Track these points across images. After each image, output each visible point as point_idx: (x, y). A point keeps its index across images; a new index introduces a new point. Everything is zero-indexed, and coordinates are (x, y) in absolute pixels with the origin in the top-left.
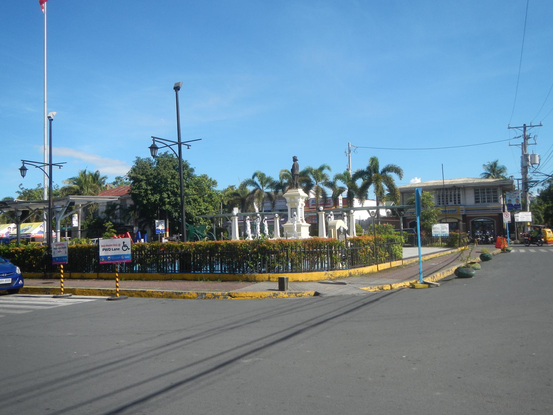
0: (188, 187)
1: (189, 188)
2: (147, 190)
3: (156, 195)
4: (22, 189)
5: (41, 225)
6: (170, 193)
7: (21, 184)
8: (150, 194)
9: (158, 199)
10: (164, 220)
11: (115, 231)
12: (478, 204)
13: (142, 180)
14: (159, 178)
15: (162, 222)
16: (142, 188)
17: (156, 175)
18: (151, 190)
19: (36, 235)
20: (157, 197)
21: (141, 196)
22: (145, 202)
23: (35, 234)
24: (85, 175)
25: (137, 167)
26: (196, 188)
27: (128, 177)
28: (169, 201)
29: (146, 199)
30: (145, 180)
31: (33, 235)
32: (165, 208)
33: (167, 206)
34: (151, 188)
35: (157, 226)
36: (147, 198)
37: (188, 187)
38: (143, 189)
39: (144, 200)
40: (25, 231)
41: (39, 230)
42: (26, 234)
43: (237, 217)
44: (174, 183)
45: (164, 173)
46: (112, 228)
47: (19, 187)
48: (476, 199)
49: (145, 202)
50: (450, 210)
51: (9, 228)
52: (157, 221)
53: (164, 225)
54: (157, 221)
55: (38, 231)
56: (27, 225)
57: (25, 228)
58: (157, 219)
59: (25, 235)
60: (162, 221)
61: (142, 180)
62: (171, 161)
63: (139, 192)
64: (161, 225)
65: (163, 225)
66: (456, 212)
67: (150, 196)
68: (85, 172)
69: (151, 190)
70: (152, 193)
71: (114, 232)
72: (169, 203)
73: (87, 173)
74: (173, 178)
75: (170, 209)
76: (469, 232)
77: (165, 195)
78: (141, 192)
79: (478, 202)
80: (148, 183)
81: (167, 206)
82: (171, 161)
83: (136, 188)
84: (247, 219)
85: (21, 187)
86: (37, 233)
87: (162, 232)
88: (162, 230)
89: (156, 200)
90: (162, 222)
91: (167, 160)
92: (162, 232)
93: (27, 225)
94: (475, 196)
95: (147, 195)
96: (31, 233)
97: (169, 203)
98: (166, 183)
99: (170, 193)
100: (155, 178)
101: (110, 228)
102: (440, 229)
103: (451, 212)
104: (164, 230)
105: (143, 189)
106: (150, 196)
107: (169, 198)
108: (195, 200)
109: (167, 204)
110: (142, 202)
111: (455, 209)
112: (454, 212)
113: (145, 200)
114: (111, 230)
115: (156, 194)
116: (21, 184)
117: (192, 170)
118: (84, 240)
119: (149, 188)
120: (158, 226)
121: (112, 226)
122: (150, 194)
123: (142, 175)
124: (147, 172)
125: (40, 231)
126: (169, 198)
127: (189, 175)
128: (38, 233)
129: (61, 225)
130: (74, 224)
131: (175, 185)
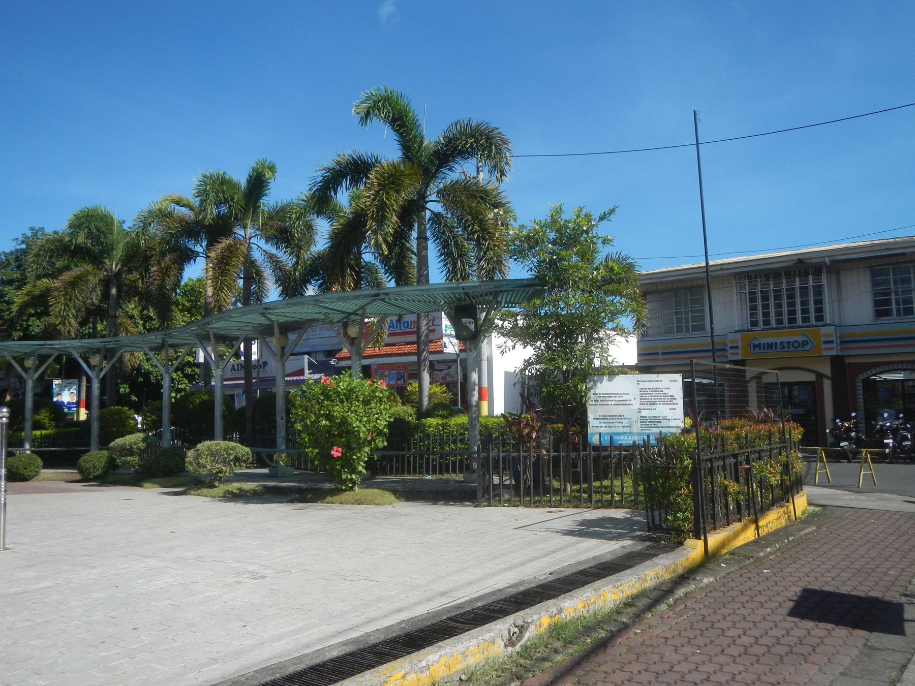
10: (76, 381)
12: (884, 320)
15: (70, 383)
35: (58, 394)
48: (877, 303)
50: (788, 343)
52: (56, 382)
53: (75, 392)
54: (56, 382)
58: (57, 377)
60: (70, 381)
64: (69, 390)
65: (74, 389)
66: (807, 348)
76: (853, 414)
79: (888, 313)
87: (69, 408)
88: (69, 403)
90: (70, 383)
92: (69, 408)
94: (875, 295)
102: (636, 405)
103: (792, 349)
104: (73, 403)
111: (805, 338)
112: (801, 349)
120: (61, 394)
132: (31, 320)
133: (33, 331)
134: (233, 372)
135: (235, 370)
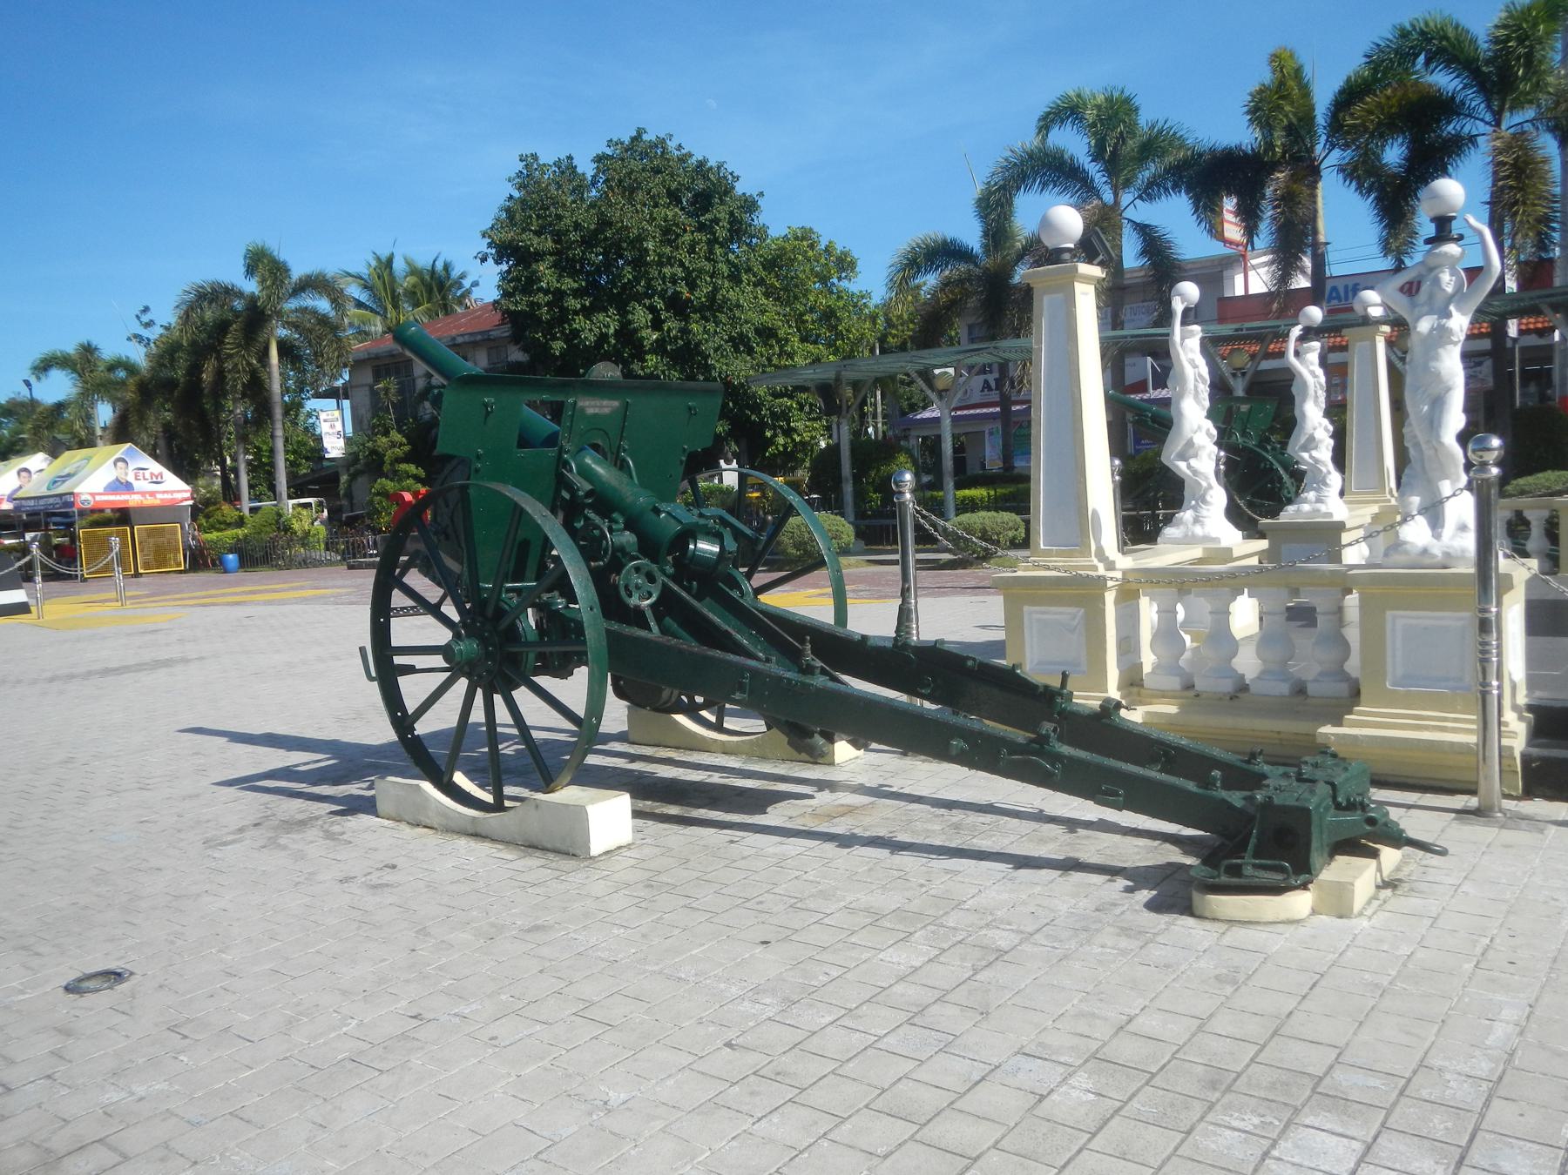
0: (735, 278)
1: (741, 282)
2: (559, 295)
3: (601, 316)
4: (148, 325)
5: (118, 455)
6: (660, 305)
7: (146, 310)
8: (576, 313)
9: (612, 331)
11: (421, 472)
13: (539, 256)
14: (606, 239)
16: (540, 289)
17: (593, 227)
18: (577, 293)
19: (98, 498)
20: (609, 322)
21: (539, 320)
22: (558, 346)
23: (93, 495)
24: (391, 274)
25: (523, 201)
26: (772, 286)
27: (489, 250)
28: (657, 340)
29: (563, 333)
30: (551, 254)
31: (83, 498)
32: (643, 369)
33: (652, 360)
34: (576, 285)
36: (565, 328)
37: (735, 278)
38: (546, 292)
39: (554, 338)
40: (64, 481)
41: (114, 478)
42: (60, 496)
43: (1096, 271)
44: (670, 261)
45: (631, 218)
46: (407, 459)
47: (138, 317)
49: (558, 346)
51: (23, 474)
55: (105, 485)
56: (76, 460)
57: (66, 471)
59: (58, 500)
61: (539, 256)
62: (657, 171)
63: (532, 304)
67: (579, 322)
68: (390, 261)
69: (577, 293)
70: (583, 306)
71: (417, 478)
72: (659, 348)
73: (399, 266)
74: (669, 234)
75: (663, 372)
77: (640, 316)
78: (539, 306)
80: (565, 265)
81: (652, 360)
82: (657, 171)
83: (515, 289)
84: (1178, 306)
85: (145, 319)
89: (603, 338)
91: (643, 170)
93: (76, 460)
95: (563, 316)
96: (76, 491)
97: (659, 348)
98: (639, 263)
99: (660, 305)
100: (589, 241)
101: (398, 460)
105: (546, 292)
106: (579, 322)
107: (657, 324)
108: (766, 333)
109: (649, 352)
110: (546, 348)
113: (558, 339)
114: (403, 466)
115: (606, 310)
116: (146, 310)
117: (750, 205)
118: (299, 513)
119: (569, 284)
121: (407, 448)
122: (576, 313)
123: (538, 233)
124: (559, 218)
125: (117, 479)
126: (657, 324)
127: (738, 229)
129: (287, 452)
130: (329, 450)
131: (679, 272)
132: (577, 321)
133: (586, 338)
134: (986, 391)
135: (990, 389)
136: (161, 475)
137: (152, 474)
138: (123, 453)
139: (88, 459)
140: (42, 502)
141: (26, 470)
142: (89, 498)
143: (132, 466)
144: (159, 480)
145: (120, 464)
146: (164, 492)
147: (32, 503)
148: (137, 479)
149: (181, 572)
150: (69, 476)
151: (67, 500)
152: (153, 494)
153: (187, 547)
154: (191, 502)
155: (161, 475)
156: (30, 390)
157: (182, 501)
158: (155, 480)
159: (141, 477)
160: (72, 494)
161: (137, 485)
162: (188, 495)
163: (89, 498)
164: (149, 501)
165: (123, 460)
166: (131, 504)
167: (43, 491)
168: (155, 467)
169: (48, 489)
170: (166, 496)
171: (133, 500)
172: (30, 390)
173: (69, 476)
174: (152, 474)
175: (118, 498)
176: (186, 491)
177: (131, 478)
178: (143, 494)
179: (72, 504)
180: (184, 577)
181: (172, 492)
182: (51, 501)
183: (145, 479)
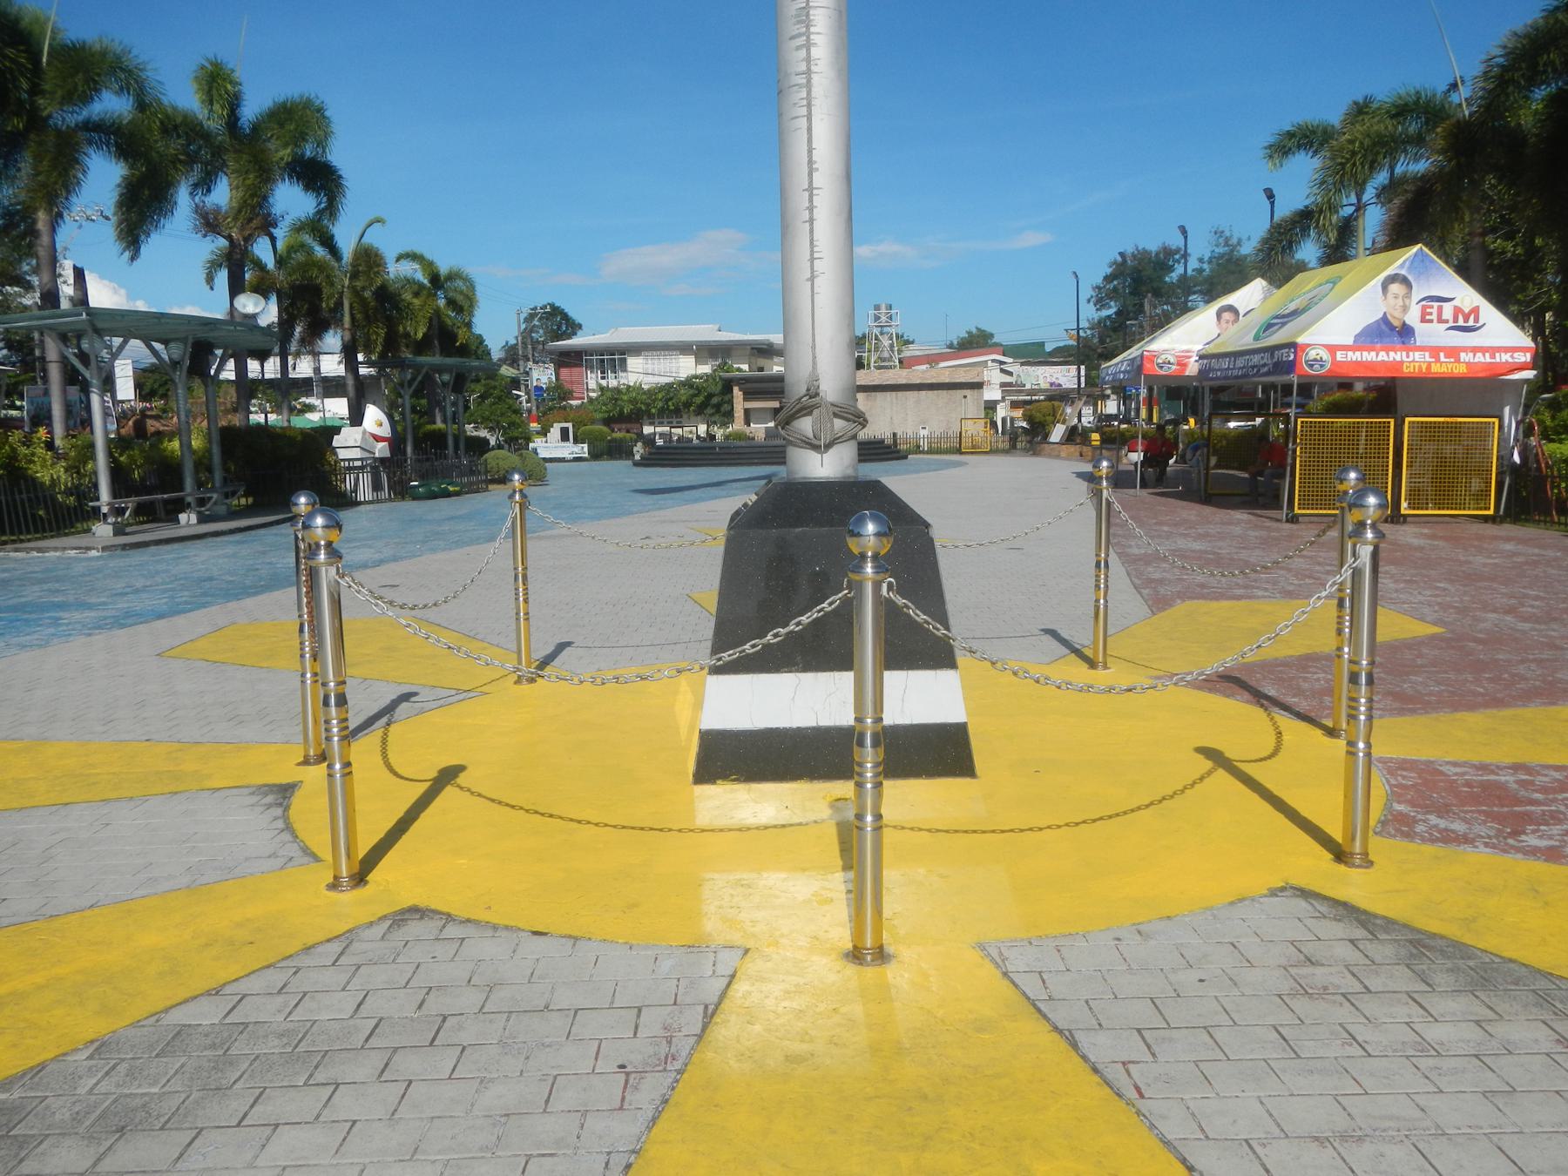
23: (1332, 349)
31: (1312, 354)
40: (1284, 324)
41: (1380, 315)
51: (1227, 316)
57: (1292, 307)
59: (1267, 359)
86: (1350, 341)
96: (1300, 340)
125: (1385, 319)
128: (1357, 337)
136: (1476, 311)
137: (1457, 311)
138: (1402, 266)
139: (1334, 282)
140: (1240, 362)
141: (1231, 309)
142: (1325, 355)
143: (1418, 294)
144: (1471, 323)
145: (1395, 288)
146: (1475, 350)
147: (1225, 364)
148: (1423, 320)
149: (1486, 519)
150: (1295, 313)
151: (1282, 358)
152: (1453, 352)
153: (1506, 467)
154: (1530, 374)
155: (1476, 311)
156: (1272, 204)
157: (1512, 371)
158: (1461, 323)
159: (1434, 317)
160: (1293, 345)
161: (1432, 334)
162: (1526, 358)
163: (1325, 355)
164: (1444, 367)
165: (1405, 281)
166: (1407, 370)
167: (1247, 342)
168: (1466, 296)
169: (1256, 338)
170: (1479, 358)
171: (1412, 362)
172: (1272, 204)
173: (1295, 313)
174: (1457, 311)
175: (1383, 356)
176: (1523, 350)
177: (1413, 318)
178: (1435, 351)
179: (1290, 367)
180: (1490, 529)
181: (1493, 351)
182: (1256, 359)
183: (1440, 321)
